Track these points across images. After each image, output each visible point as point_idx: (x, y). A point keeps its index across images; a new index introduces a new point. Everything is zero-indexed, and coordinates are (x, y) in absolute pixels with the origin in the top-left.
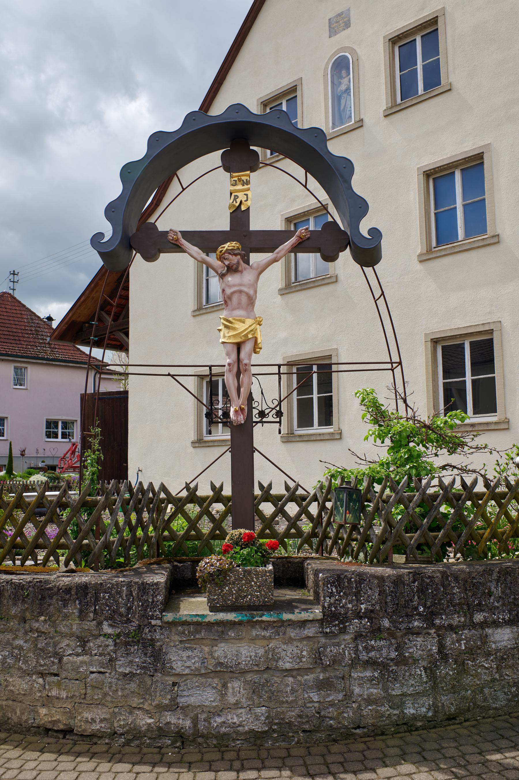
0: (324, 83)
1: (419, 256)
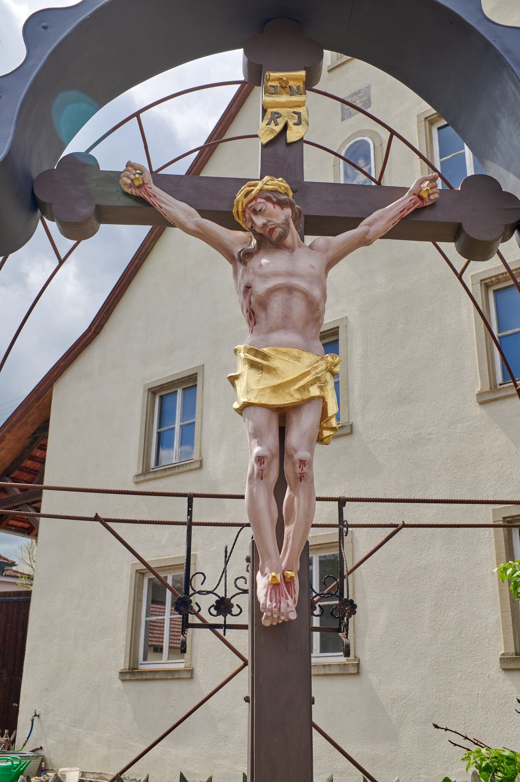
0: (334, 175)
1: (480, 395)
